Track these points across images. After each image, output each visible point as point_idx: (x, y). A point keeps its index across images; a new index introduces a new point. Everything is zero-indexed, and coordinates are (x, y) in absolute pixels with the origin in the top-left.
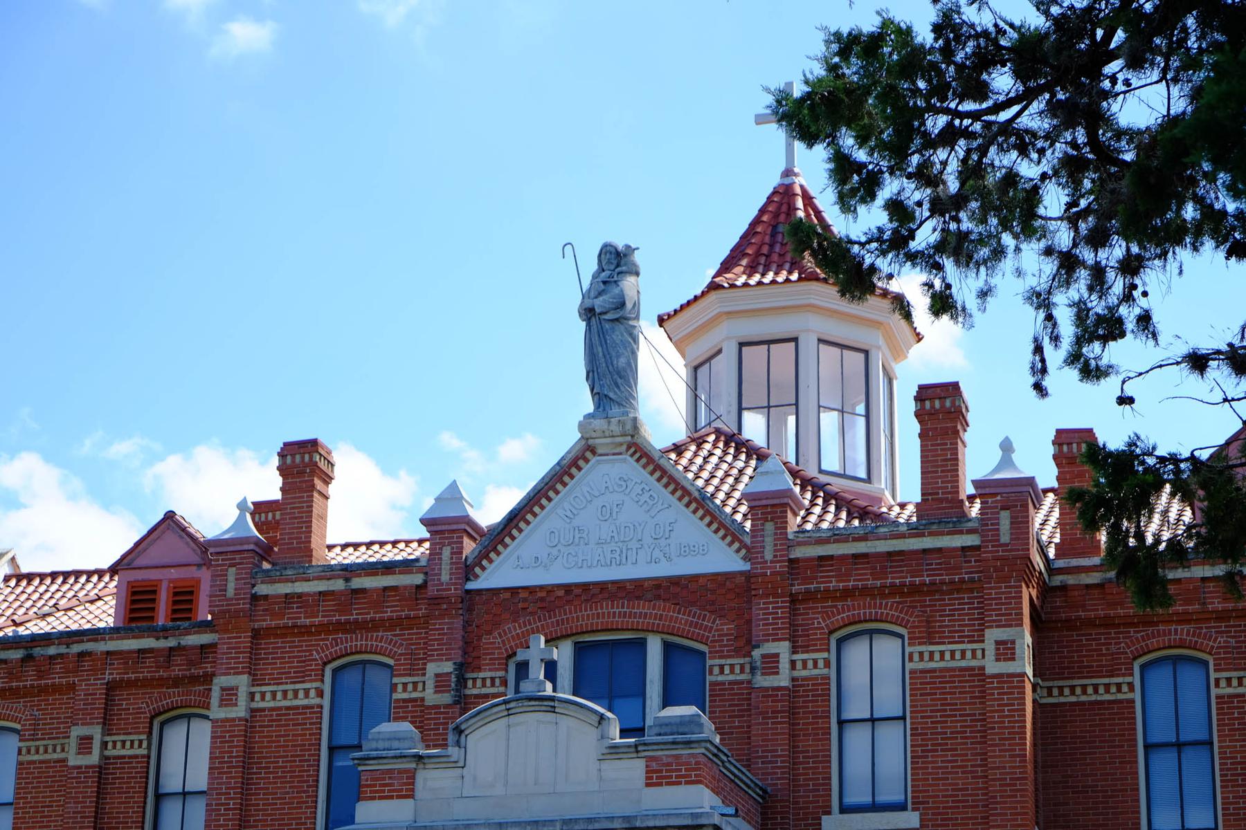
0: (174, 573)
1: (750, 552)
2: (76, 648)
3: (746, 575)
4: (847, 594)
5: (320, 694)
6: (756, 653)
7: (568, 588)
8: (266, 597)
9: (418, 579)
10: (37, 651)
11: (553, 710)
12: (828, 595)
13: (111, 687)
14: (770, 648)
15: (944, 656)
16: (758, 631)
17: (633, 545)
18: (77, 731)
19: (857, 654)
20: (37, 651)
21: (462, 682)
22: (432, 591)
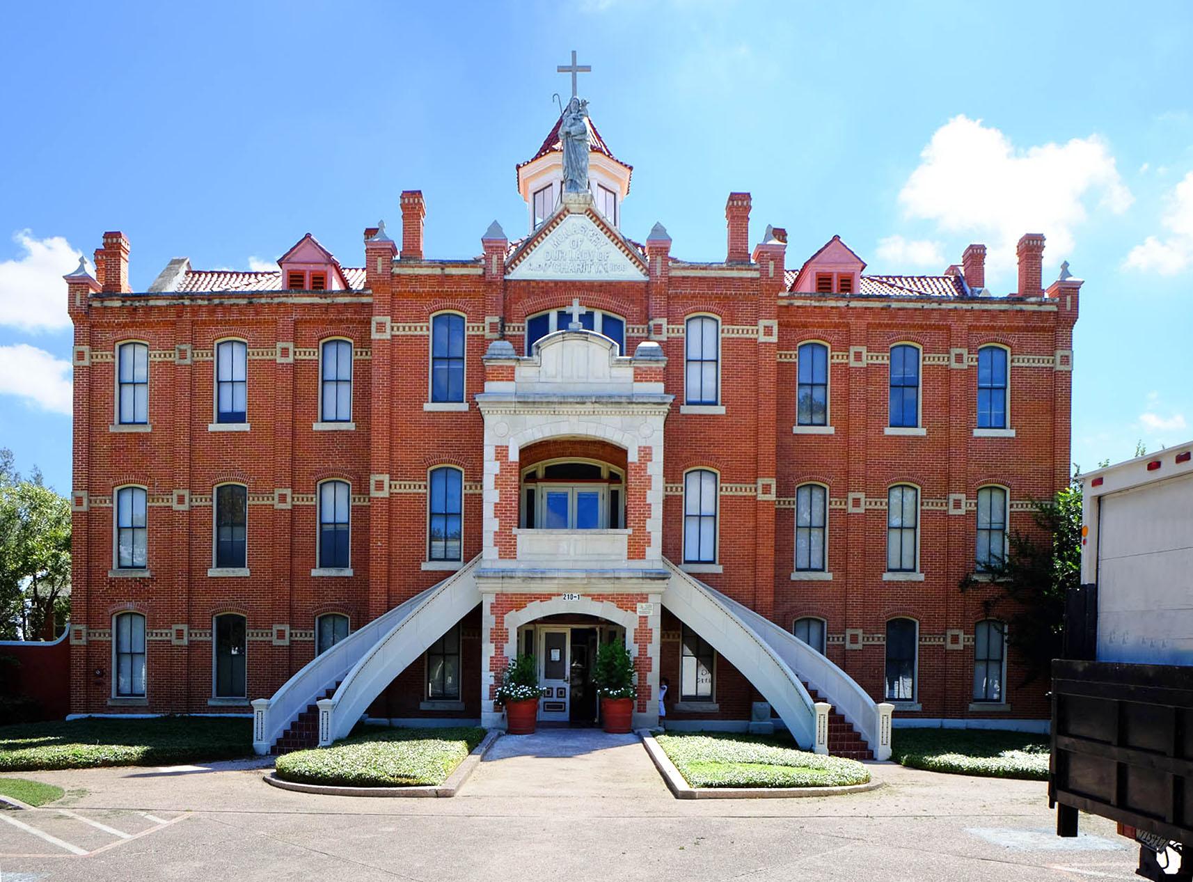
0: (312, 267)
1: (649, 272)
2: (276, 300)
3: (648, 282)
4: (694, 296)
5: (428, 329)
6: (651, 323)
7: (556, 283)
8: (399, 275)
9: (480, 271)
10: (254, 300)
11: (586, 339)
12: (685, 296)
13: (296, 323)
14: (658, 321)
15: (740, 331)
16: (652, 312)
17: (589, 262)
18: (280, 345)
19: (695, 327)
20: (254, 300)
21: (503, 326)
22: (488, 278)
